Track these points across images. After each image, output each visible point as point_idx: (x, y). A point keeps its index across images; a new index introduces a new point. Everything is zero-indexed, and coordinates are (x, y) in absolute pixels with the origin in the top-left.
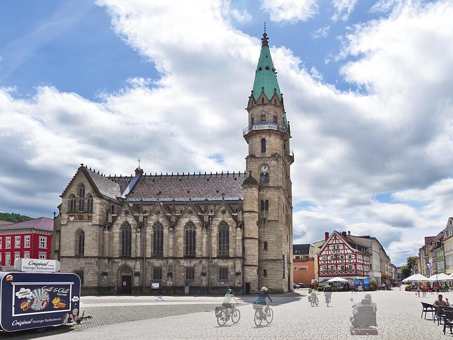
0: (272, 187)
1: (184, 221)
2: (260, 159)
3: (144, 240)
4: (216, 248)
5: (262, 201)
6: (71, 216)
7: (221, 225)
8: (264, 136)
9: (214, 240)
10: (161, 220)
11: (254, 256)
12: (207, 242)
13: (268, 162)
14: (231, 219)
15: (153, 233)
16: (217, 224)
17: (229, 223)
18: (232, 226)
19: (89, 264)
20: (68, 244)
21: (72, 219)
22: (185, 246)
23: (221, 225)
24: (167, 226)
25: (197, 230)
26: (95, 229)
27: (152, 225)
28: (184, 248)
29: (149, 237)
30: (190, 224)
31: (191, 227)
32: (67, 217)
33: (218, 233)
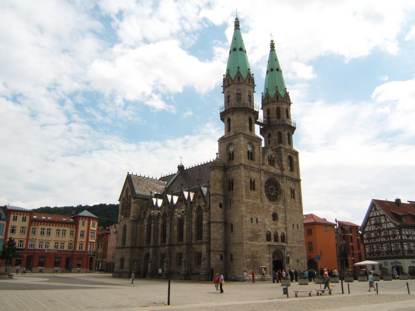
0: (235, 166)
3: (156, 229)
4: (194, 234)
5: (229, 181)
6: (122, 215)
7: (199, 210)
9: (194, 226)
11: (216, 240)
12: (187, 228)
15: (163, 223)
16: (196, 210)
22: (179, 233)
23: (199, 210)
28: (177, 235)
29: (160, 227)
33: (197, 219)
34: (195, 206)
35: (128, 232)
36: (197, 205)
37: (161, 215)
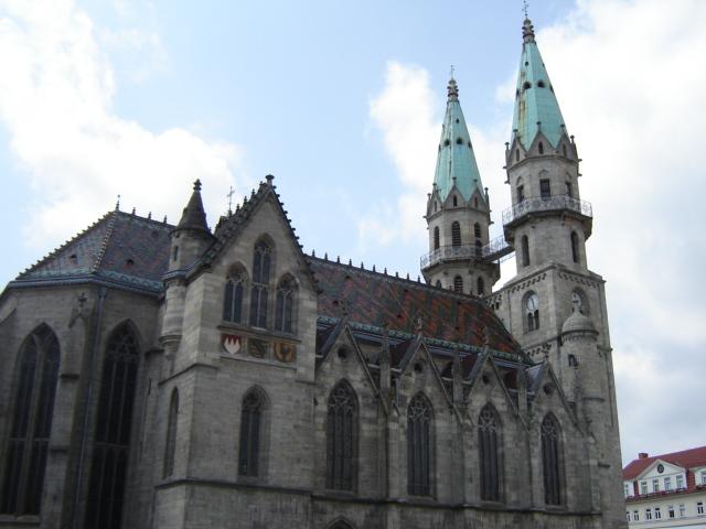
1: (477, 401)
2: (574, 277)
6: (230, 337)
8: (574, 227)
10: (429, 390)
13: (584, 287)
14: (562, 411)
16: (541, 420)
17: (561, 421)
18: (566, 430)
19: (283, 512)
20: (215, 437)
21: (233, 348)
24: (442, 411)
25: (505, 431)
26: (300, 394)
27: (408, 401)
30: (489, 409)
31: (487, 421)
32: (218, 339)
34: (539, 410)
35: (280, 426)
36: (544, 408)
37: (405, 398)
